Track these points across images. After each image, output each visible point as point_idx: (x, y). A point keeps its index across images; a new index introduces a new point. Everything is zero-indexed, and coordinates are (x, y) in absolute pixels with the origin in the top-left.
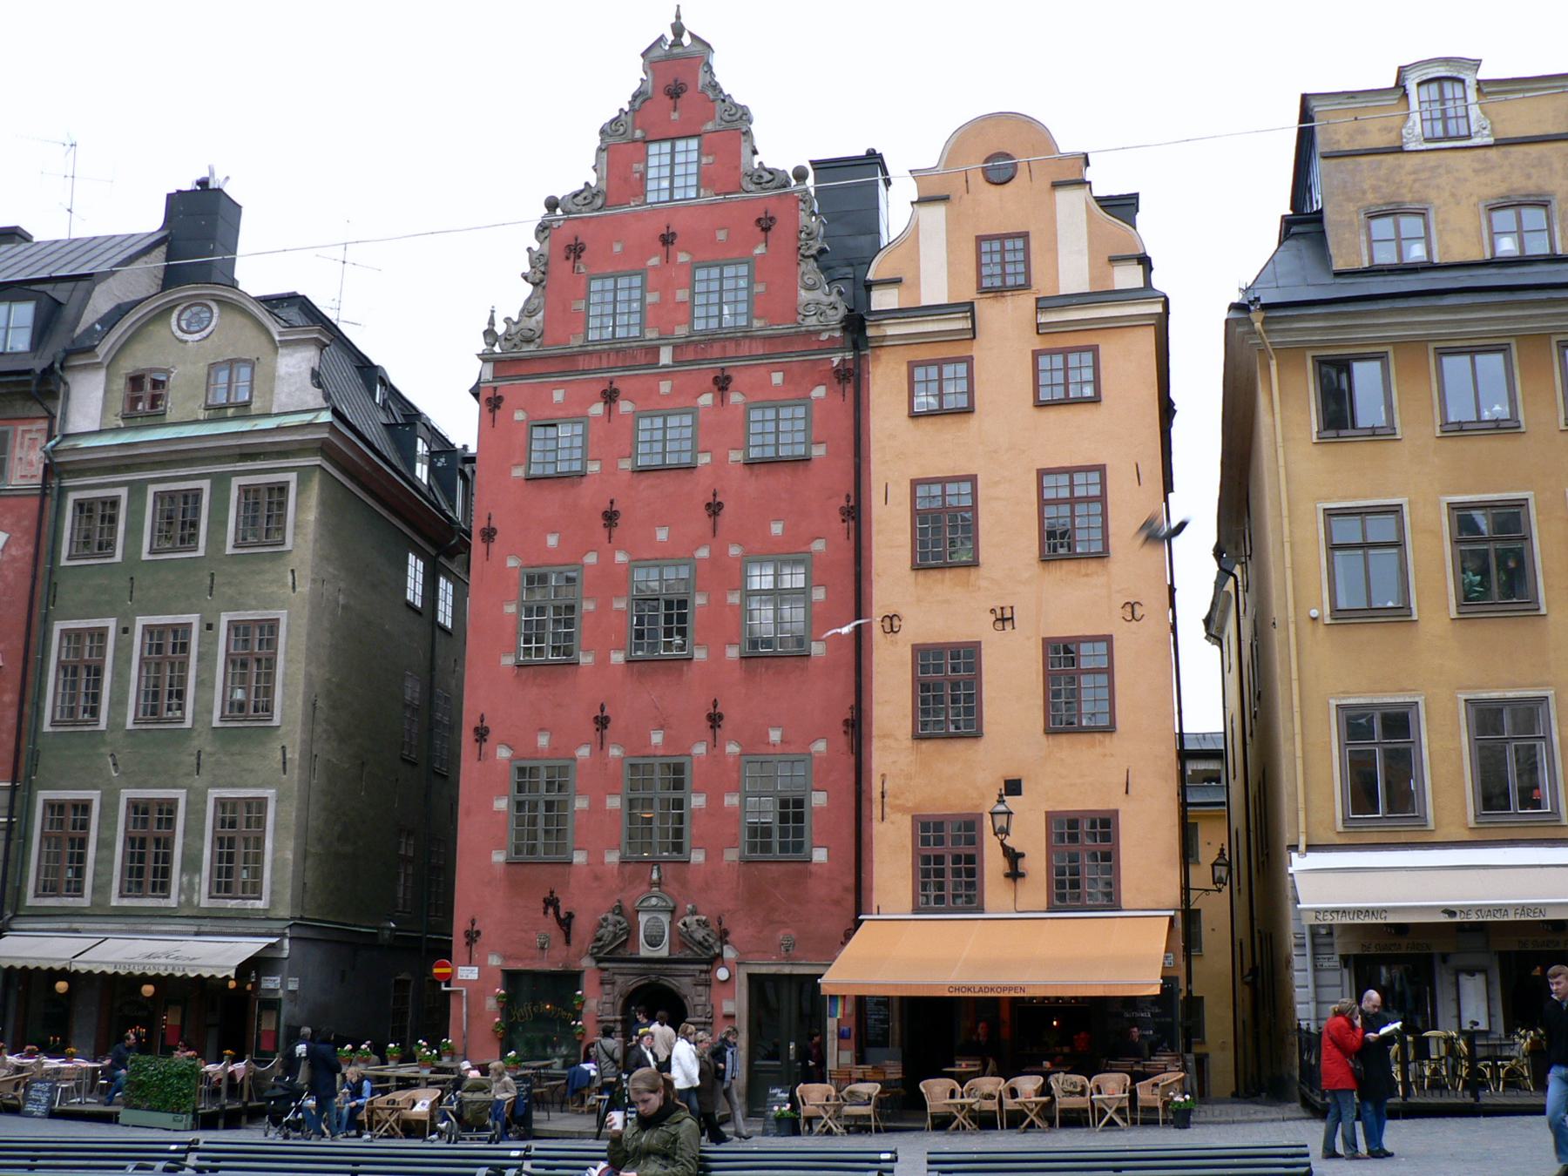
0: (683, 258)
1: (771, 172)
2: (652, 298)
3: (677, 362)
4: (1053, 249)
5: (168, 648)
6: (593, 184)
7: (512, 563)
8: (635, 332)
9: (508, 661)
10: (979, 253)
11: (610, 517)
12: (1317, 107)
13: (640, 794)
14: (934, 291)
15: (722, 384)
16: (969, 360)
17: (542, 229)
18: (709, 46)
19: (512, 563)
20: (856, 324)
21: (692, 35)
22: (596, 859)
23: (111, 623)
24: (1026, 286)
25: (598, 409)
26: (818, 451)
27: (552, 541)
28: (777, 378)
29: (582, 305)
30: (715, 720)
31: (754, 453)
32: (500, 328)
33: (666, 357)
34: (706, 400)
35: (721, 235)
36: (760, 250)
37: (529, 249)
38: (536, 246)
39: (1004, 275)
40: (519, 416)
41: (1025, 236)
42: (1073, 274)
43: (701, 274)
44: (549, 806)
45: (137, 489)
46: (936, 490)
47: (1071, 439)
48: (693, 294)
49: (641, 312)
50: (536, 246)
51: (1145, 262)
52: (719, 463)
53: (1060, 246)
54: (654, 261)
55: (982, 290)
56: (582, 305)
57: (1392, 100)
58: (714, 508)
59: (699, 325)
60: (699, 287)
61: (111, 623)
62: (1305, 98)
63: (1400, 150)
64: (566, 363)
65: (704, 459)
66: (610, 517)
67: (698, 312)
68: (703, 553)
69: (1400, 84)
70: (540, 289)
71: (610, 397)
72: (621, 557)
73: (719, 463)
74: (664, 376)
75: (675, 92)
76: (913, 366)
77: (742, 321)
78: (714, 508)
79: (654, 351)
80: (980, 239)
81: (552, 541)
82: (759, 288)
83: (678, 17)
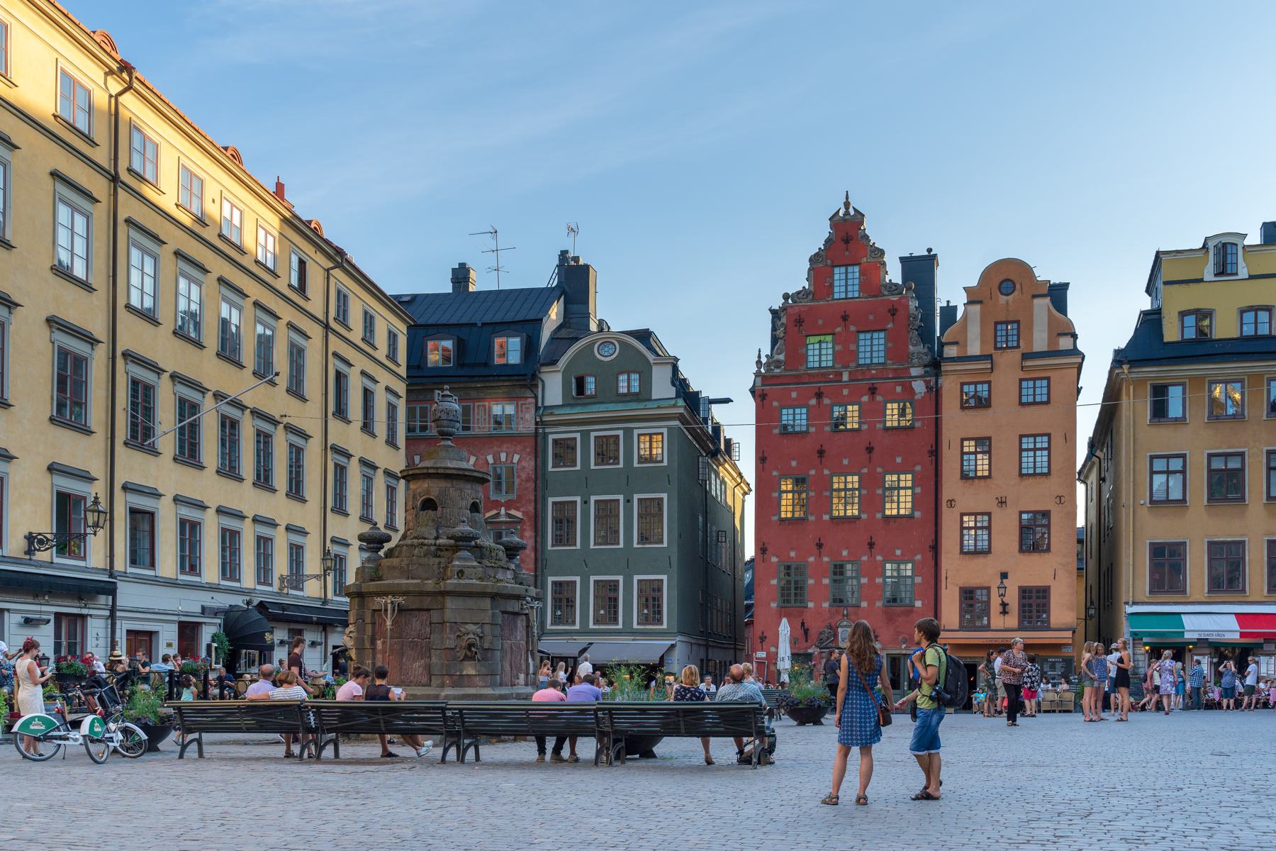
0: (853, 328)
2: (838, 348)
3: (851, 380)
4: (1031, 329)
5: (607, 512)
7: (775, 473)
8: (830, 364)
9: (775, 518)
10: (996, 330)
11: (821, 453)
12: (1164, 258)
13: (793, 571)
14: (974, 349)
15: (873, 391)
16: (989, 383)
19: (775, 473)
20: (935, 365)
23: (578, 499)
24: (1018, 347)
25: (813, 402)
26: (918, 424)
27: (794, 464)
28: (899, 389)
29: (803, 351)
31: (889, 424)
32: (764, 360)
33: (845, 377)
34: (865, 399)
35: (871, 317)
36: (890, 326)
39: (1007, 341)
40: (775, 404)
41: (1018, 322)
42: (1040, 341)
43: (862, 336)
45: (585, 435)
48: (858, 346)
49: (834, 354)
51: (1075, 336)
52: (872, 426)
53: (1035, 329)
54: (839, 329)
55: (996, 348)
56: (803, 351)
57: (1200, 254)
59: (861, 362)
60: (862, 343)
61: (578, 499)
62: (1158, 253)
63: (1201, 280)
64: (797, 380)
65: (865, 427)
66: (821, 453)
67: (861, 355)
68: (865, 470)
69: (1204, 246)
71: (819, 395)
72: (826, 472)
73: (872, 426)
74: (845, 386)
76: (962, 384)
77: (882, 360)
78: (870, 450)
79: (841, 374)
80: (996, 323)
81: (794, 464)
82: (890, 345)
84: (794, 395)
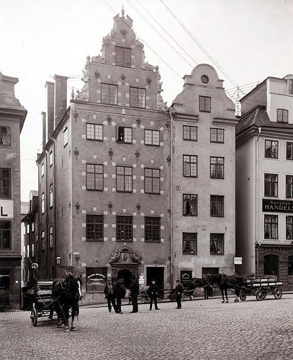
1: (150, 66)
6: (101, 55)
17: (89, 66)
18: (132, 21)
21: (127, 16)
22: (110, 240)
25: (105, 123)
30: (138, 207)
32: (75, 92)
37: (83, 71)
38: (85, 71)
44: (97, 226)
46: (188, 157)
47: (218, 150)
50: (85, 71)
55: (200, 111)
58: (137, 155)
70: (88, 83)
75: (124, 33)
83: (123, 8)
84: (94, 117)
